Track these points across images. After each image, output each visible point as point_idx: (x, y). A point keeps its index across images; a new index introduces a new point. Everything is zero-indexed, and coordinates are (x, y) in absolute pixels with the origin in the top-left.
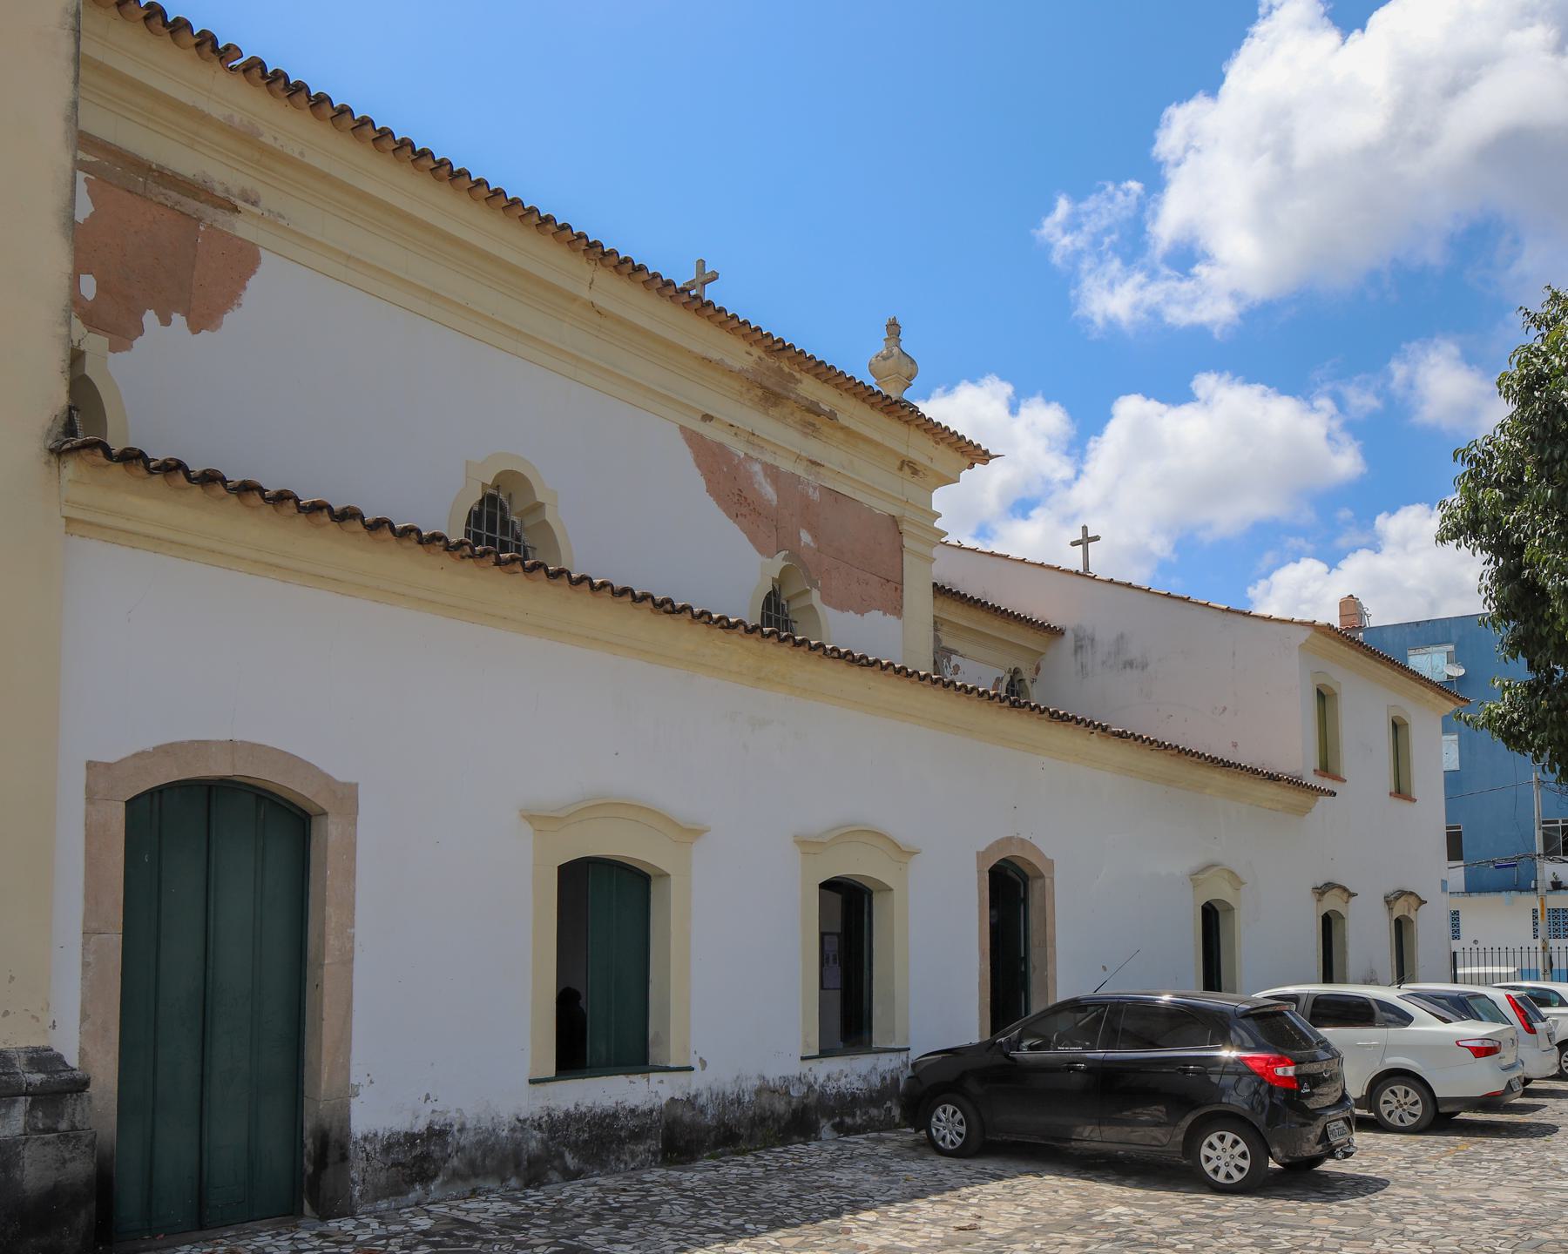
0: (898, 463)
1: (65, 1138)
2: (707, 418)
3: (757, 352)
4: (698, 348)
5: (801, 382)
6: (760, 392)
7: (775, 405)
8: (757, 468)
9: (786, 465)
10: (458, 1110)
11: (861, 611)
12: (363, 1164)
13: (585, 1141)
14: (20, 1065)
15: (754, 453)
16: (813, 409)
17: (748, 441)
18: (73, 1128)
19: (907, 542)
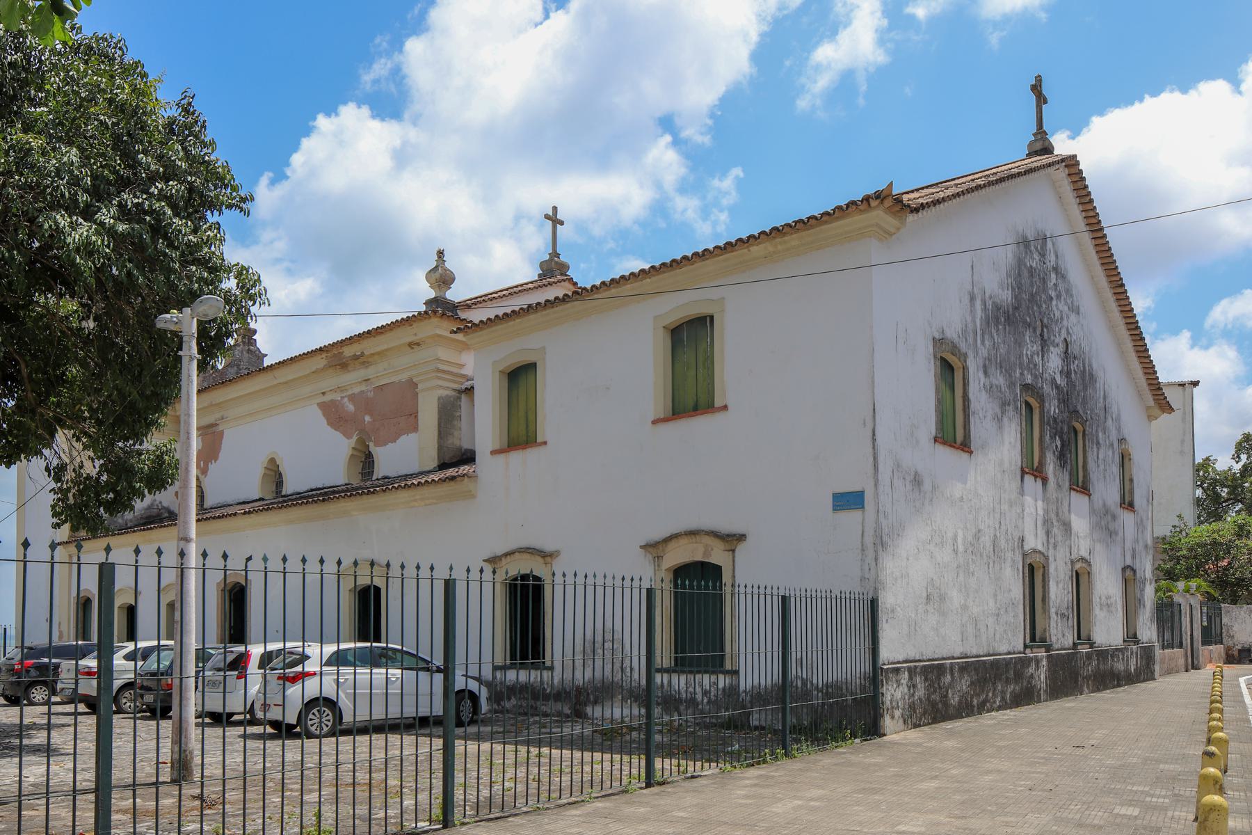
3: (324, 355)
4: (308, 372)
6: (338, 367)
8: (346, 400)
9: (357, 390)
16: (356, 358)
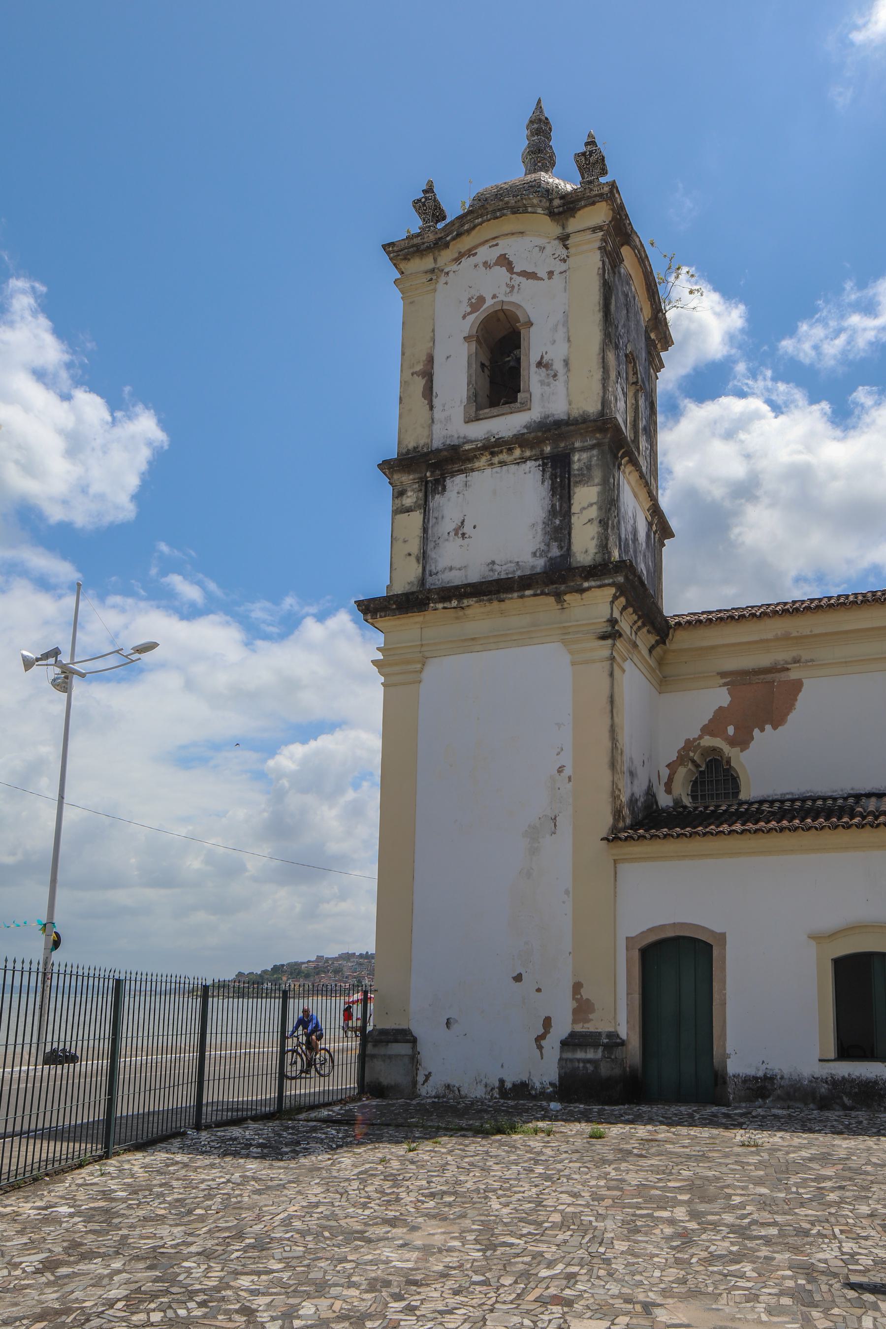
1: (613, 1060)
10: (780, 1069)
12: (733, 1086)
13: (856, 1093)
14: (604, 1036)
18: (616, 1058)
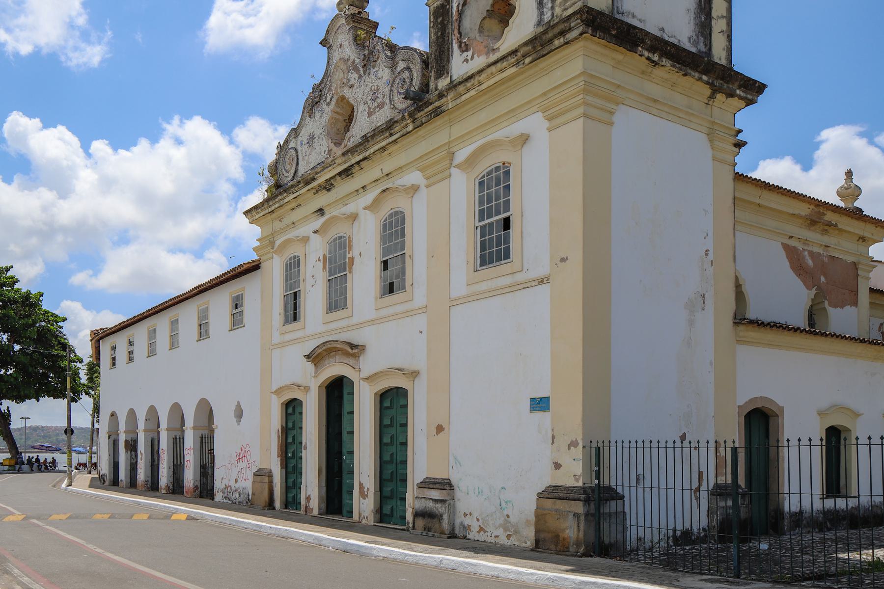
0: (858, 238)
2: (791, 237)
3: (812, 207)
5: (826, 214)
7: (814, 225)
8: (806, 253)
9: (816, 250)
11: (842, 307)
15: (805, 248)
16: (829, 224)
17: (803, 243)
19: (860, 272)
